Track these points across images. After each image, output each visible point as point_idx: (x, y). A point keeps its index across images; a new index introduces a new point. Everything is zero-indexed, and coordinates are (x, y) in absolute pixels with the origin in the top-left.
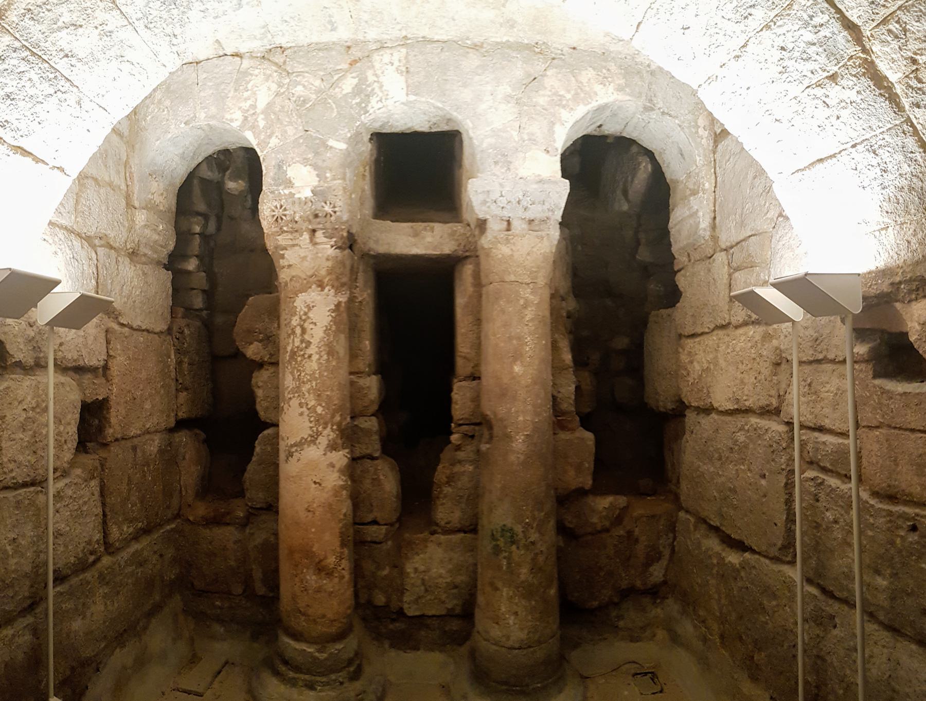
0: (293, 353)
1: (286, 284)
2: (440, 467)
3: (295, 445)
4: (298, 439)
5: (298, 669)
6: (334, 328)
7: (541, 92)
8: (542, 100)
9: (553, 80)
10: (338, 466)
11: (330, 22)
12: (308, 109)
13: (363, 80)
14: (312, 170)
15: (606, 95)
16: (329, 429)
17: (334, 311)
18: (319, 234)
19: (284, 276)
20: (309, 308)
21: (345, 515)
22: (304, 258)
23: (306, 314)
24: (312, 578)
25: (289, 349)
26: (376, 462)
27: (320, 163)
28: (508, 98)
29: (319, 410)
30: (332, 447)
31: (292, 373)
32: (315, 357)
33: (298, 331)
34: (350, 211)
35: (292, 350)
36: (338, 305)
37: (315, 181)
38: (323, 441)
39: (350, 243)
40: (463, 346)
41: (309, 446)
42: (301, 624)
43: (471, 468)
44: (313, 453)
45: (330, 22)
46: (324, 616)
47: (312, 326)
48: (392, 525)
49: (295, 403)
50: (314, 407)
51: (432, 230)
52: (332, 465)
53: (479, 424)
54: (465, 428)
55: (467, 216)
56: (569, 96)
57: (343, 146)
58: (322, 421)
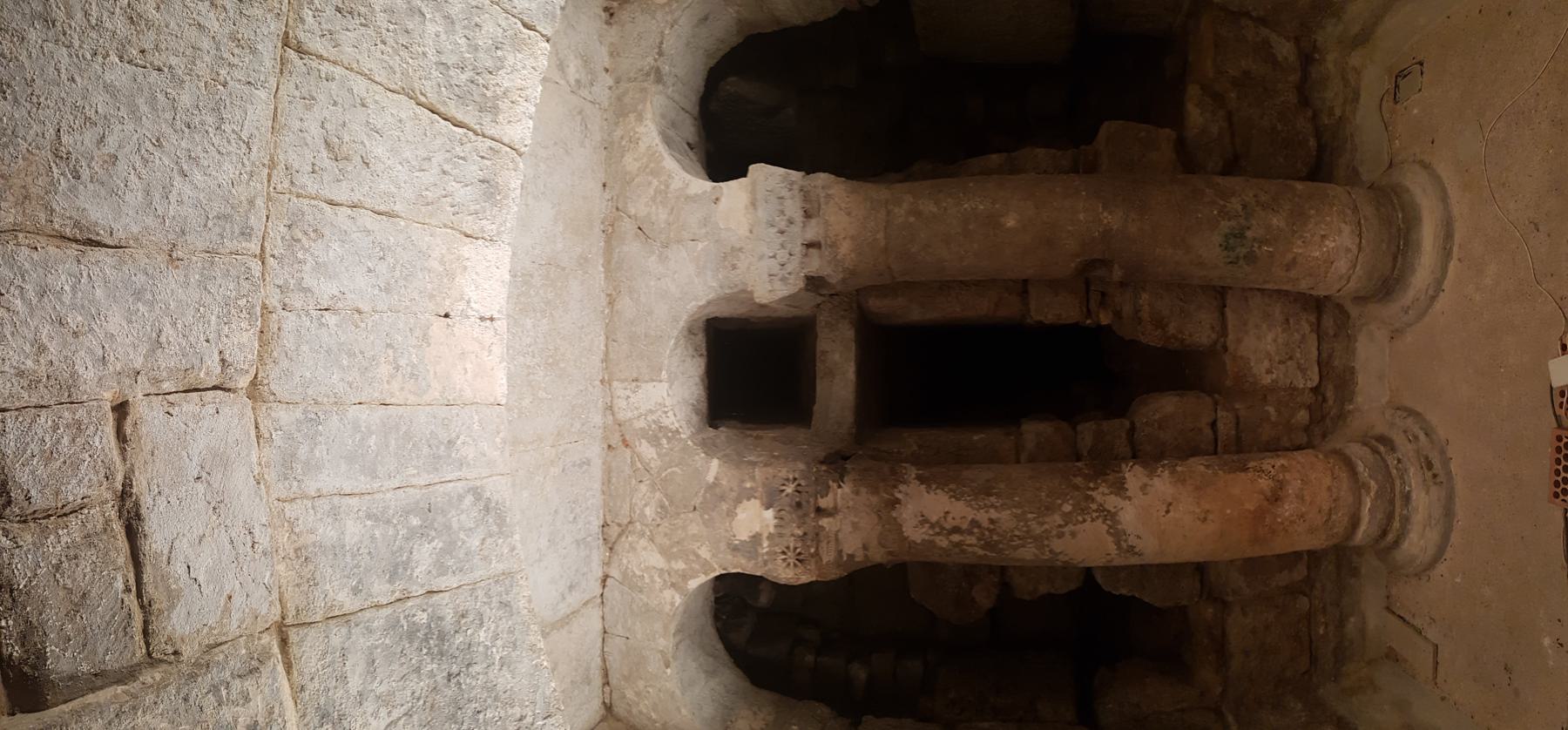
0: (988, 546)
1: (890, 553)
2: (1142, 339)
3: (1118, 543)
4: (1110, 539)
5: (1390, 517)
6: (952, 486)
7: (654, 218)
8: (662, 215)
9: (639, 206)
10: (1146, 480)
11: (580, 466)
12: (671, 502)
13: (643, 434)
14: (741, 506)
15: (649, 133)
16: (1094, 494)
17: (929, 487)
18: (824, 503)
19: (878, 556)
20: (925, 521)
21: (1207, 467)
22: (855, 526)
23: (932, 526)
24: (1287, 509)
25: (981, 552)
26: (1138, 425)
27: (734, 494)
28: (663, 259)
29: (1067, 508)
30: (1120, 488)
31: (1016, 548)
32: (993, 514)
33: (956, 538)
34: (795, 460)
35: (982, 548)
36: (921, 479)
37: (754, 505)
38: (1112, 502)
39: (836, 462)
40: (978, 307)
41: (1119, 522)
42: (1341, 519)
43: (1145, 296)
44: (1129, 515)
45: (580, 466)
46: (1329, 489)
47: (949, 519)
48: (1216, 403)
49: (1057, 545)
50: (1066, 515)
51: (824, 353)
52: (1144, 488)
53: (1087, 283)
54: (1093, 305)
55: (805, 310)
56: (655, 182)
57: (715, 463)
58: (1083, 504)
